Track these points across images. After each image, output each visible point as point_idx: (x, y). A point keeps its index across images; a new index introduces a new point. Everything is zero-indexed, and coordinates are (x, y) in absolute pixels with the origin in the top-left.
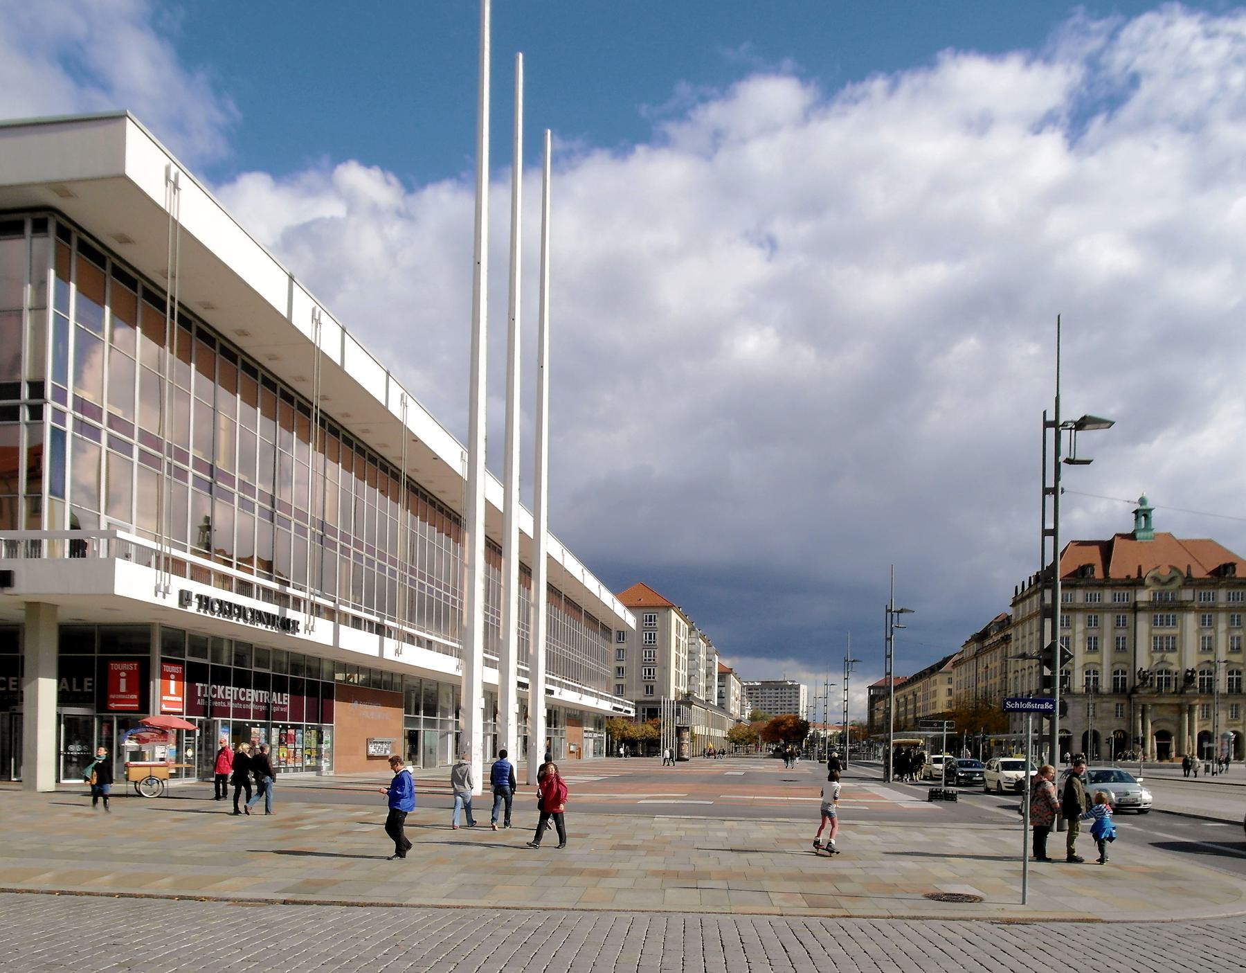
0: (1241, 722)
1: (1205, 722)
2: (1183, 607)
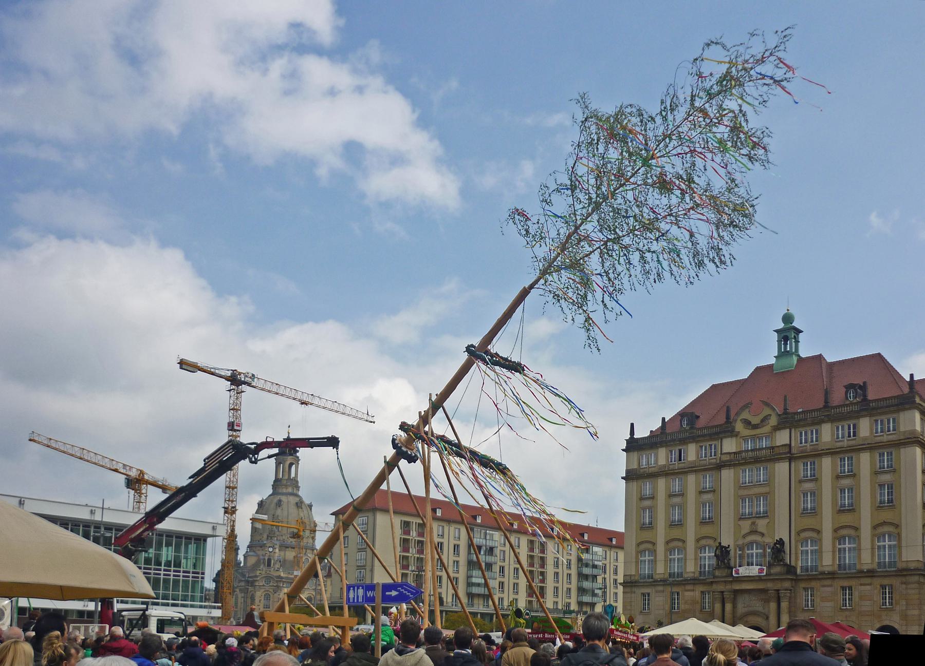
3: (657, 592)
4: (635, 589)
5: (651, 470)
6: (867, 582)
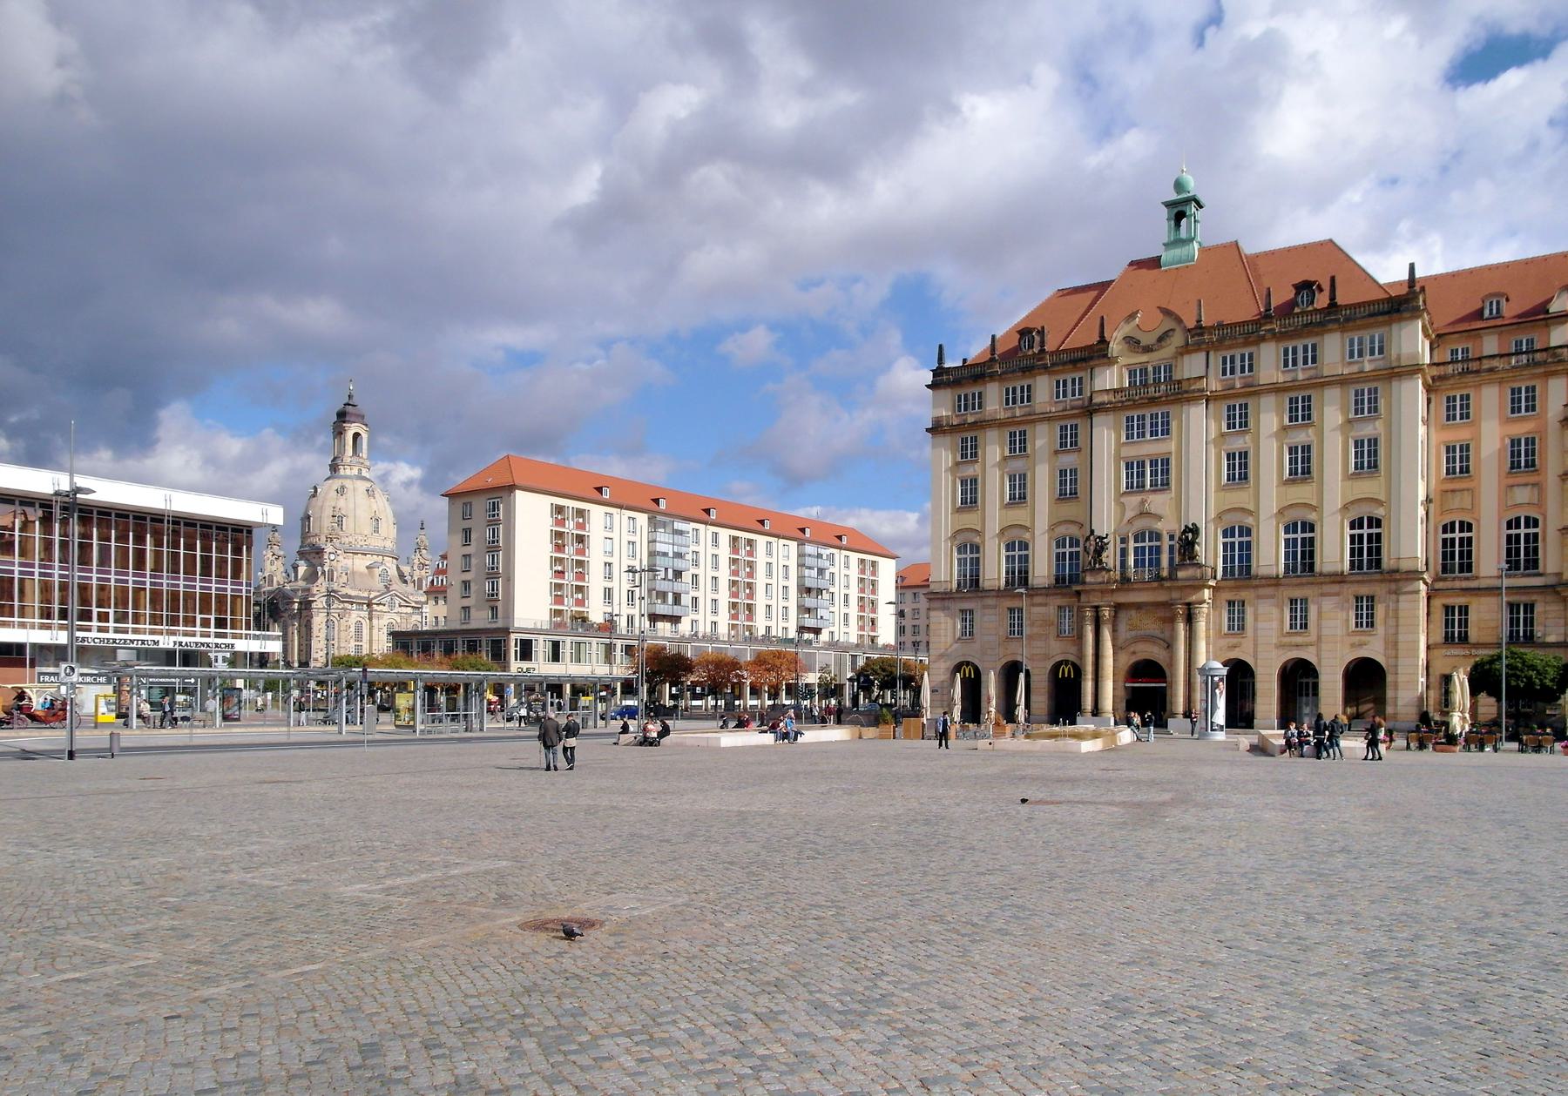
0: (1313, 638)
1: (1234, 641)
2: (1182, 394)
3: (984, 607)
6: (1332, 591)
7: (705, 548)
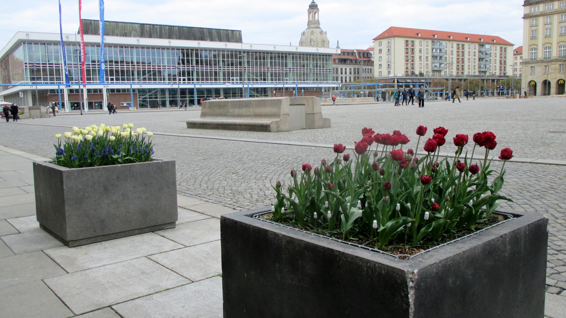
3: (538, 66)
4: (527, 65)
5: (536, 14)
7: (449, 49)
